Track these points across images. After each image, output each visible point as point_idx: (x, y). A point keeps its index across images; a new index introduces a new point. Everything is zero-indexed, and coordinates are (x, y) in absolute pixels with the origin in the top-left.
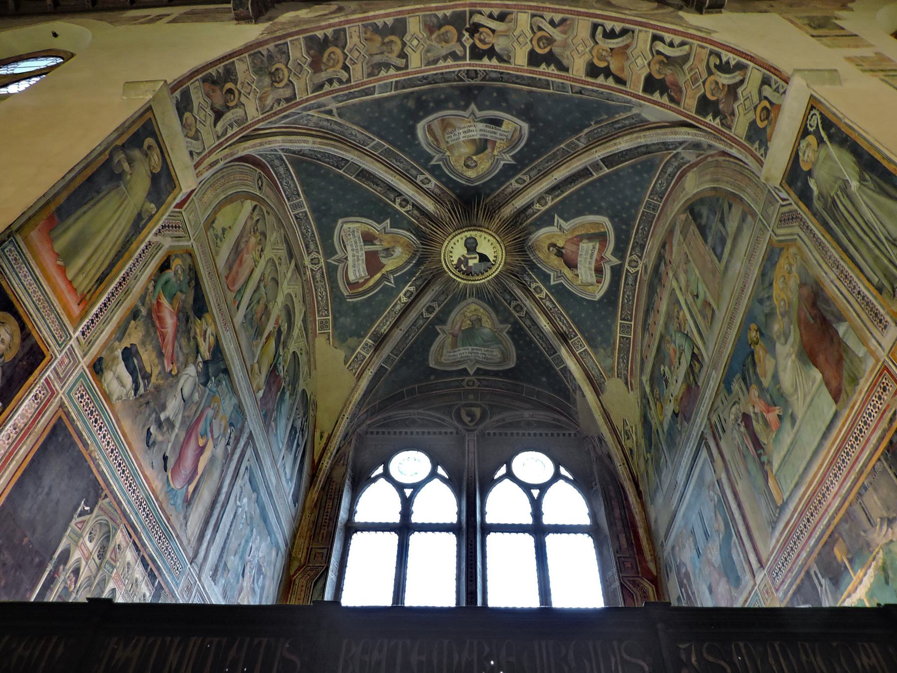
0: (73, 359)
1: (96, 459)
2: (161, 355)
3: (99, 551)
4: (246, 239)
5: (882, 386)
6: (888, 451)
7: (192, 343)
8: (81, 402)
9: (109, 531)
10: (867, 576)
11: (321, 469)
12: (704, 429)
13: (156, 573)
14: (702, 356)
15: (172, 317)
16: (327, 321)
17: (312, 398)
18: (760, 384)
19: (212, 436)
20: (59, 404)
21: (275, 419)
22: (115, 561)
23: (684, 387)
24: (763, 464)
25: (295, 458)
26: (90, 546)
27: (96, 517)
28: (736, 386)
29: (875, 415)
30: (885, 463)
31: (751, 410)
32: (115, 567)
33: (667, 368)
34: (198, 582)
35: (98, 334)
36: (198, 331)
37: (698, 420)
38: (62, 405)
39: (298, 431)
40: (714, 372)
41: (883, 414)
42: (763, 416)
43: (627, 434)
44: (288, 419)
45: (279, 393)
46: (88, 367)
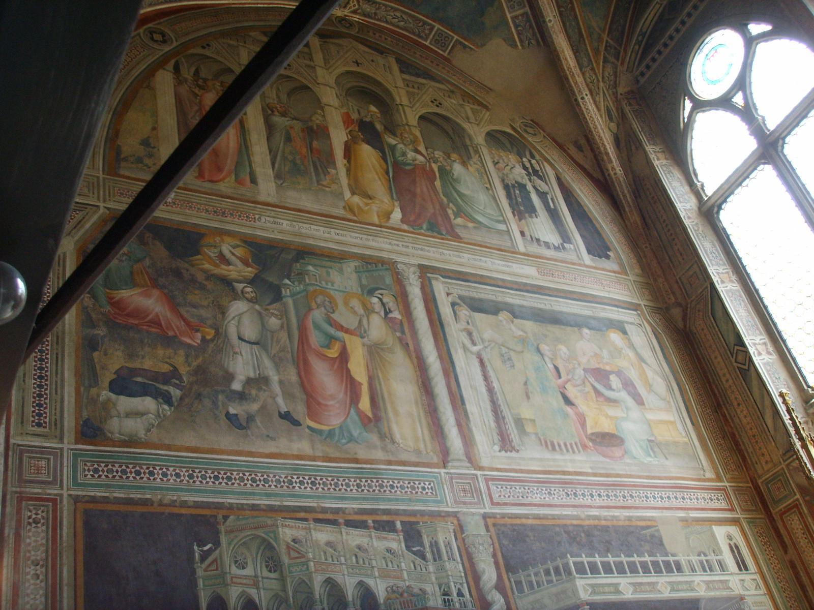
0: (50, 453)
1: (176, 501)
2: (170, 341)
3: (267, 566)
4: (196, 108)
7: (210, 285)
8: (100, 476)
9: (264, 540)
11: (612, 182)
13: (385, 518)
15: (149, 296)
16: (440, 33)
17: (517, 126)
19: (347, 331)
20: (72, 502)
21: (459, 212)
22: (303, 557)
25: (554, 215)
26: (249, 571)
27: (229, 544)
32: (309, 560)
34: (479, 473)
35: (58, 407)
36: (207, 266)
38: (76, 500)
39: (525, 181)
44: (490, 188)
45: (438, 183)
46: (76, 443)
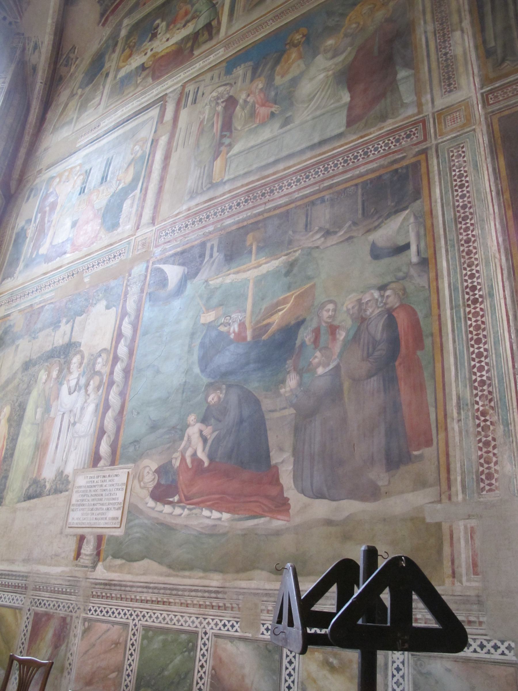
5: (408, 133)
6: (371, 183)
10: (267, 265)
12: (171, 92)
14: (218, 31)
18: (271, 79)
23: (173, 48)
24: (221, 144)
28: (239, 71)
29: (382, 151)
30: (360, 191)
31: (243, 96)
33: (164, 24)
37: (170, 82)
40: (223, 49)
41: (390, 154)
42: (253, 106)
43: (67, 61)
